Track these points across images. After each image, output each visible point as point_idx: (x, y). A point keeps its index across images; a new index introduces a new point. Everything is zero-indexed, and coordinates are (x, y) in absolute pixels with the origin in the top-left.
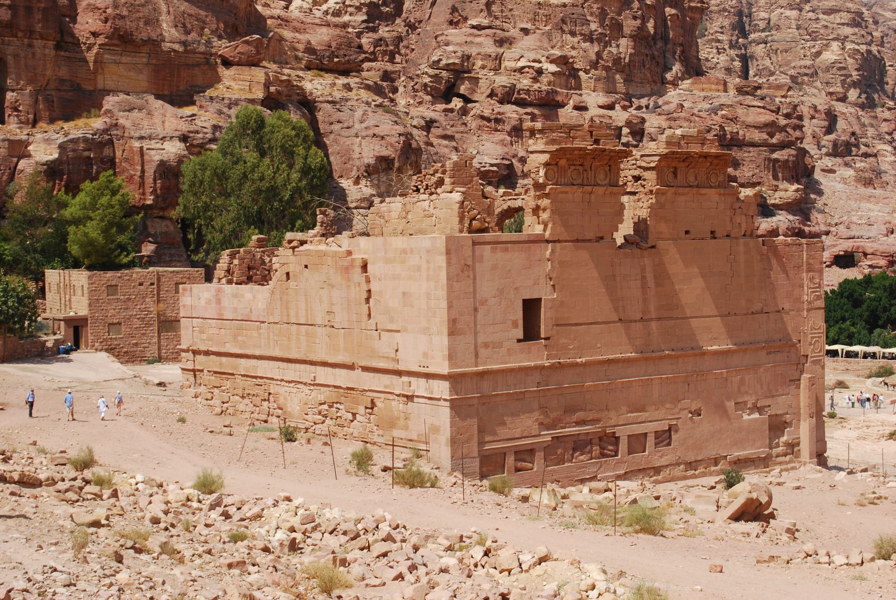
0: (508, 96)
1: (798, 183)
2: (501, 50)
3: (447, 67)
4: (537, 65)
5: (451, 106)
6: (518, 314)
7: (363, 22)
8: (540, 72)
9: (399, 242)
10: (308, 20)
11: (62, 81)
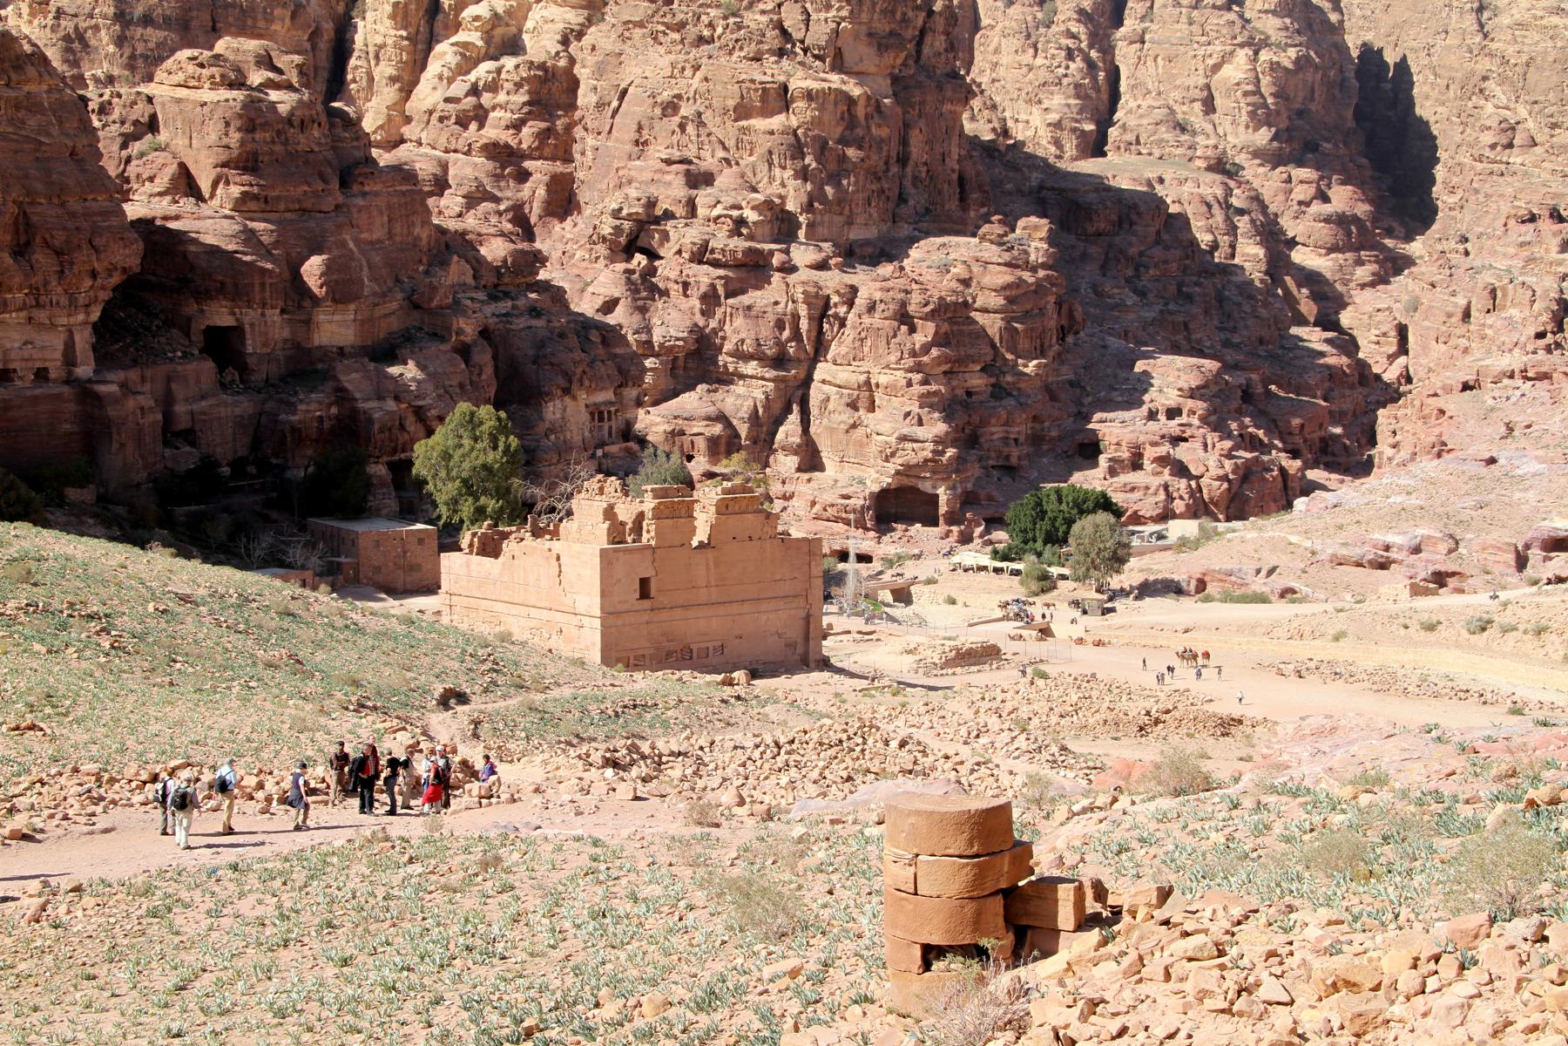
0: (701, 255)
1: (1042, 354)
2: (695, 192)
3: (629, 217)
4: (735, 213)
5: (635, 262)
6: (637, 586)
7: (524, 104)
8: (741, 222)
9: (576, 547)
10: (484, 231)
11: (286, 341)
